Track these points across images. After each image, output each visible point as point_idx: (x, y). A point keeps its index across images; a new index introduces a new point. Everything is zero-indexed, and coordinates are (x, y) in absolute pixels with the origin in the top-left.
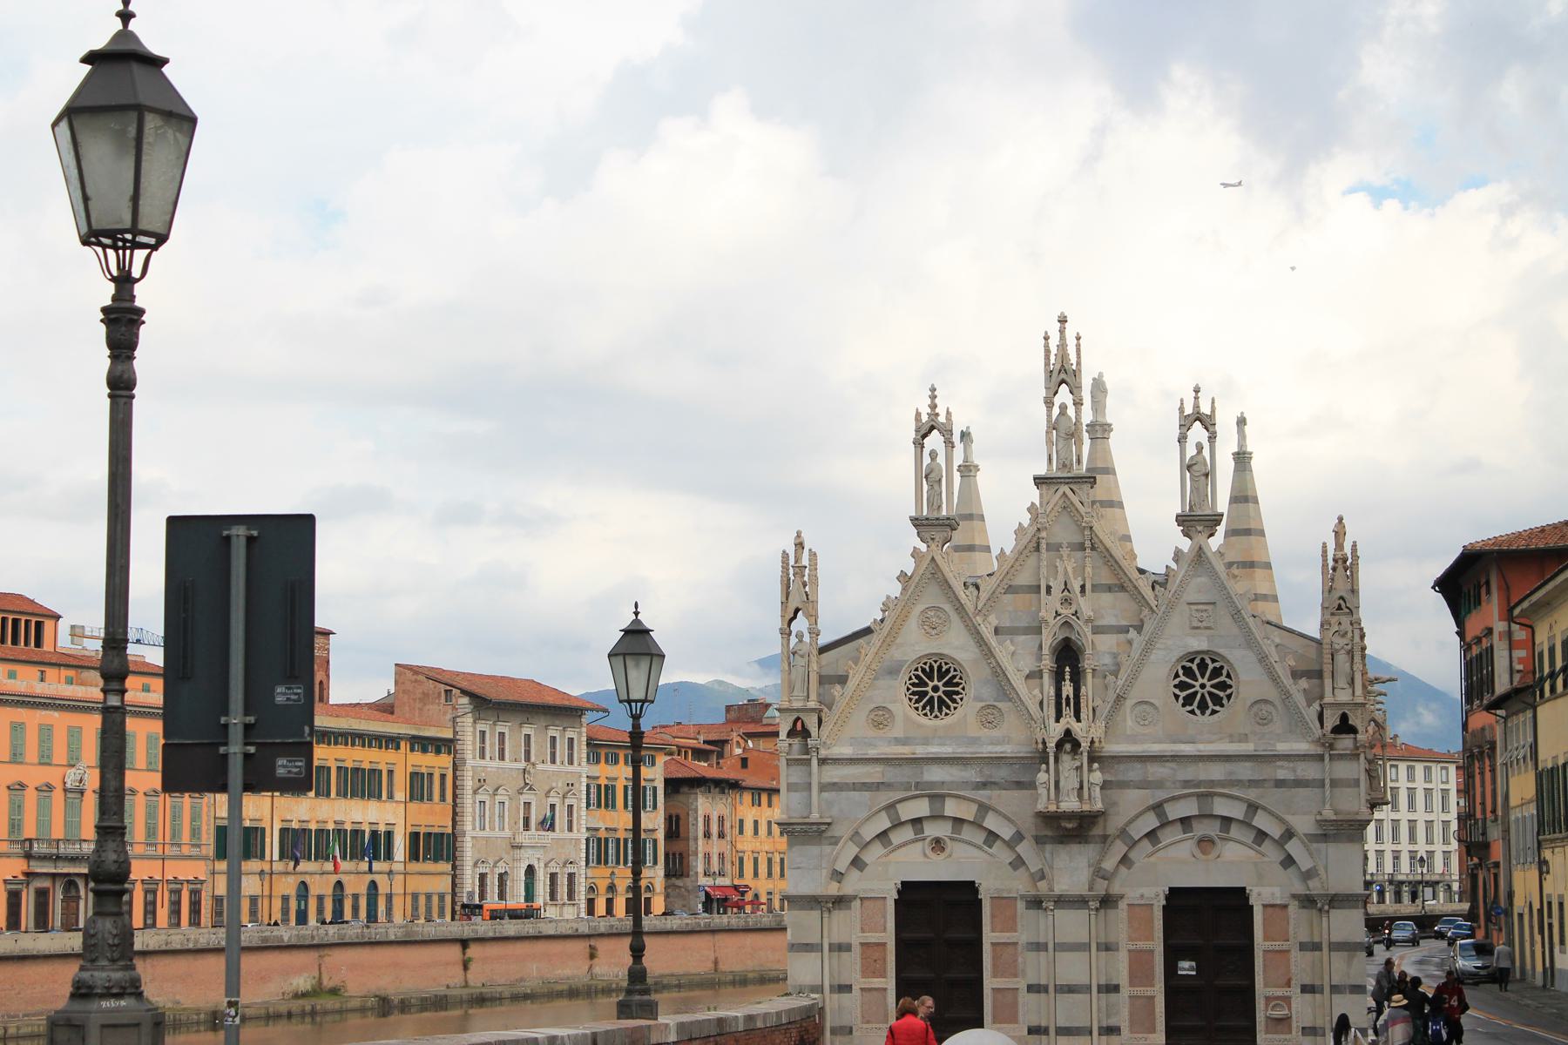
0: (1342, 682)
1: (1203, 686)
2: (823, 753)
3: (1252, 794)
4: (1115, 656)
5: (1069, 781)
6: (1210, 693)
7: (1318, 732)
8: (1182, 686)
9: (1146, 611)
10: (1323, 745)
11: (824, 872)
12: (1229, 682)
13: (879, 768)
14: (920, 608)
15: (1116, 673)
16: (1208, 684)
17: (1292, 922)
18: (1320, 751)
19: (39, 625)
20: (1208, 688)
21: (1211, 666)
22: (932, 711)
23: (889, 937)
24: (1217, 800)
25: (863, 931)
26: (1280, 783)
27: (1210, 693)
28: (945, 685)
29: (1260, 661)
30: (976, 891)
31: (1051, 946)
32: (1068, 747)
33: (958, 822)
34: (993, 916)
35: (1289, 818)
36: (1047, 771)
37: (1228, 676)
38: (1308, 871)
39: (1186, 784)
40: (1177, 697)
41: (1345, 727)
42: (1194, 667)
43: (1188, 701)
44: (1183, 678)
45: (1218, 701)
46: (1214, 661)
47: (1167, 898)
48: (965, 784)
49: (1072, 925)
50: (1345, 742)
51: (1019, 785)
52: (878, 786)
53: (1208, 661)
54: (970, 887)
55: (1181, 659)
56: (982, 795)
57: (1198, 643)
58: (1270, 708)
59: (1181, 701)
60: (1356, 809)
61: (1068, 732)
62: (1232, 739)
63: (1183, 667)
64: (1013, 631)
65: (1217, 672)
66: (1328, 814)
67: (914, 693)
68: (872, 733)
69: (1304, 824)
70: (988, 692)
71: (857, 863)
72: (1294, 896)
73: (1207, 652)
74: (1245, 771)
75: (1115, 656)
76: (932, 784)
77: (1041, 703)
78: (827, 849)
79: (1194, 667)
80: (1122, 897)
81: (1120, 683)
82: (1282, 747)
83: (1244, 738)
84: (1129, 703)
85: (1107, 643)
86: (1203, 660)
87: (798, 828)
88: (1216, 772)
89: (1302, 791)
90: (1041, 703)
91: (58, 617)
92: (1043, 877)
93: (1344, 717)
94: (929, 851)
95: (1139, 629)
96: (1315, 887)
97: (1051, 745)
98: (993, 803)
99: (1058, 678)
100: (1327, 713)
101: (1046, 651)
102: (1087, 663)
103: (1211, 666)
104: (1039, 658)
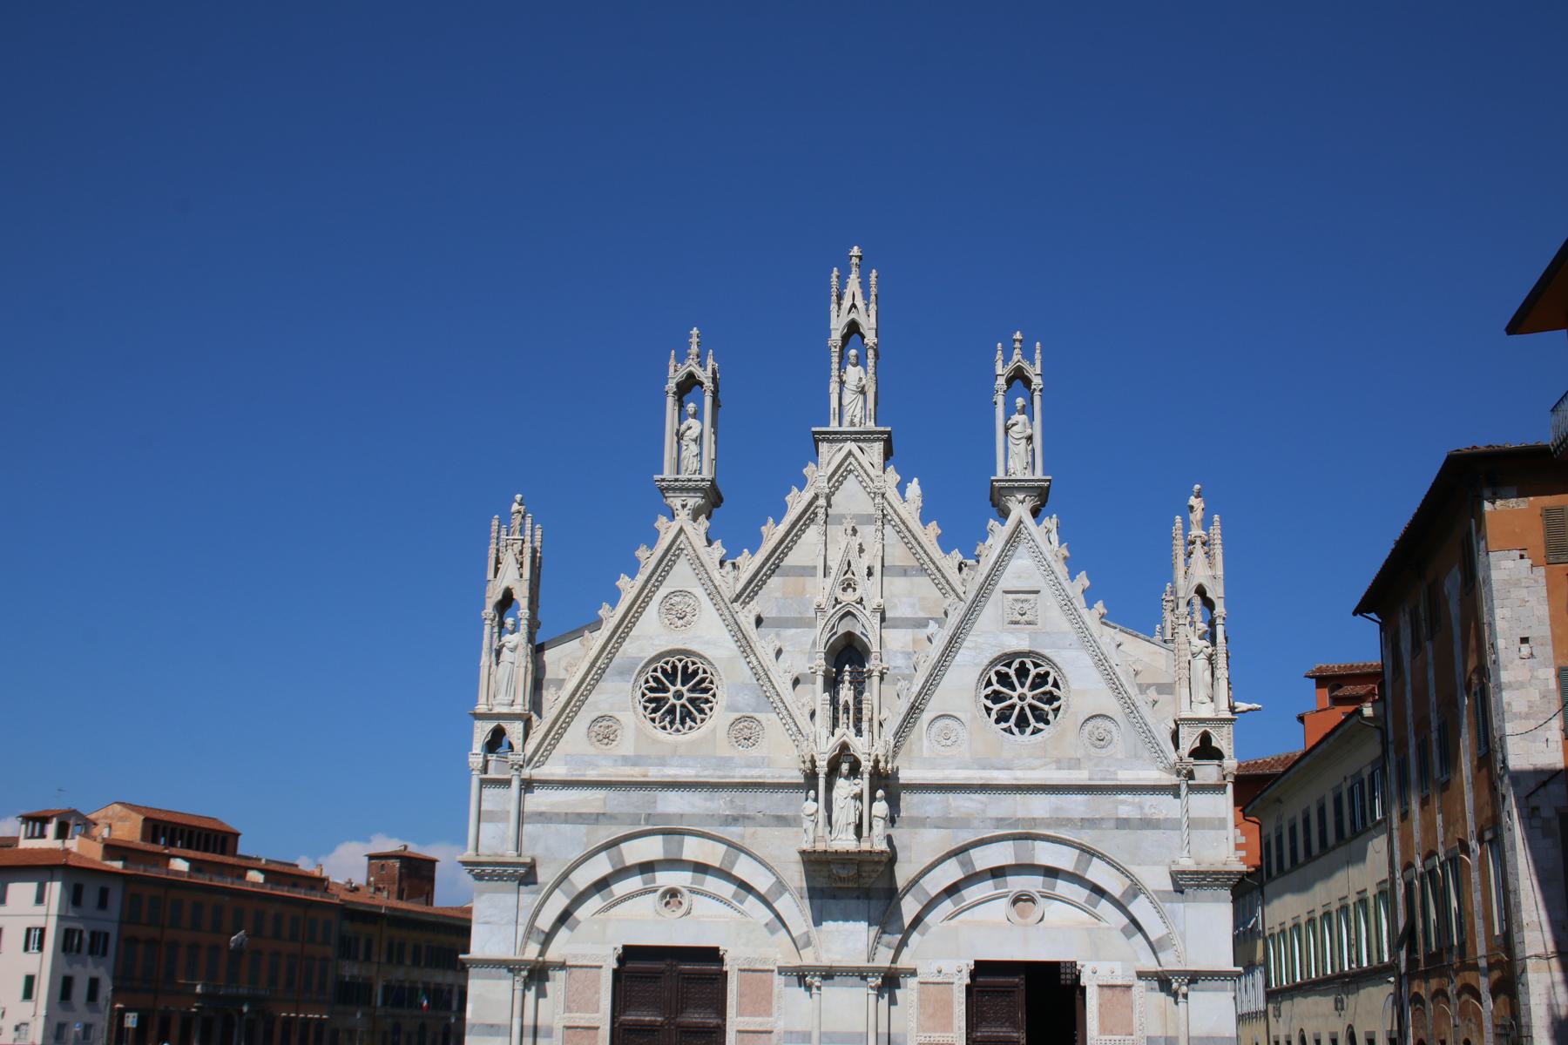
0: (1202, 693)
1: (1022, 698)
2: (527, 772)
3: (1086, 837)
4: (908, 655)
5: (845, 810)
6: (1032, 707)
7: (1173, 757)
8: (996, 697)
9: (952, 598)
10: (1179, 773)
11: (521, 930)
12: (1056, 692)
13: (599, 794)
14: (663, 591)
15: (909, 678)
16: (1030, 695)
17: (1137, 1010)
18: (1172, 779)
19: (224, 840)
20: (1029, 700)
21: (1033, 672)
22: (672, 722)
23: (602, 1016)
24: (1038, 844)
25: (568, 1009)
26: (1123, 823)
27: (1031, 706)
28: (691, 690)
29: (1097, 666)
30: (721, 960)
31: (815, 1036)
32: (845, 767)
33: (701, 868)
34: (741, 995)
35: (1133, 869)
36: (816, 800)
37: (1056, 685)
38: (1160, 940)
39: (1000, 822)
40: (988, 710)
41: (1206, 751)
42: (1012, 672)
43: (1002, 717)
44: (997, 687)
45: (1042, 718)
46: (1036, 665)
47: (973, 975)
48: (711, 818)
49: (849, 1006)
50: (1207, 772)
51: (782, 821)
52: (597, 818)
53: (1030, 666)
54: (712, 955)
55: (993, 663)
56: (732, 833)
57: (1017, 642)
58: (1108, 724)
59: (994, 716)
60: (1223, 857)
61: (844, 747)
62: (1059, 764)
63: (997, 673)
64: (782, 623)
65: (1042, 679)
66: (1187, 864)
67: (650, 700)
68: (591, 750)
69: (1157, 879)
70: (746, 700)
71: (564, 917)
72: (1141, 975)
73: (1028, 654)
74: (1077, 805)
75: (908, 655)
76: (667, 817)
77: (813, 715)
78: (529, 898)
79: (1012, 672)
80: (913, 973)
81: (916, 689)
82: (1126, 777)
83: (1075, 764)
84: (926, 717)
85: (897, 639)
86: (1022, 664)
87: (489, 869)
88: (1039, 806)
89: (1150, 835)
90: (813, 715)
91: (237, 835)
92: (808, 944)
93: (1206, 738)
94: (660, 906)
95: (940, 623)
96: (1170, 962)
97: (822, 767)
98: (747, 844)
99: (832, 684)
100: (1183, 731)
101: (821, 649)
102: (872, 664)
103: (1033, 672)
104: (811, 659)
